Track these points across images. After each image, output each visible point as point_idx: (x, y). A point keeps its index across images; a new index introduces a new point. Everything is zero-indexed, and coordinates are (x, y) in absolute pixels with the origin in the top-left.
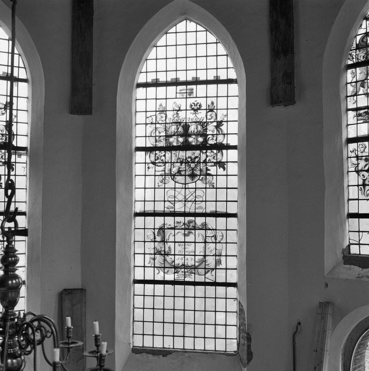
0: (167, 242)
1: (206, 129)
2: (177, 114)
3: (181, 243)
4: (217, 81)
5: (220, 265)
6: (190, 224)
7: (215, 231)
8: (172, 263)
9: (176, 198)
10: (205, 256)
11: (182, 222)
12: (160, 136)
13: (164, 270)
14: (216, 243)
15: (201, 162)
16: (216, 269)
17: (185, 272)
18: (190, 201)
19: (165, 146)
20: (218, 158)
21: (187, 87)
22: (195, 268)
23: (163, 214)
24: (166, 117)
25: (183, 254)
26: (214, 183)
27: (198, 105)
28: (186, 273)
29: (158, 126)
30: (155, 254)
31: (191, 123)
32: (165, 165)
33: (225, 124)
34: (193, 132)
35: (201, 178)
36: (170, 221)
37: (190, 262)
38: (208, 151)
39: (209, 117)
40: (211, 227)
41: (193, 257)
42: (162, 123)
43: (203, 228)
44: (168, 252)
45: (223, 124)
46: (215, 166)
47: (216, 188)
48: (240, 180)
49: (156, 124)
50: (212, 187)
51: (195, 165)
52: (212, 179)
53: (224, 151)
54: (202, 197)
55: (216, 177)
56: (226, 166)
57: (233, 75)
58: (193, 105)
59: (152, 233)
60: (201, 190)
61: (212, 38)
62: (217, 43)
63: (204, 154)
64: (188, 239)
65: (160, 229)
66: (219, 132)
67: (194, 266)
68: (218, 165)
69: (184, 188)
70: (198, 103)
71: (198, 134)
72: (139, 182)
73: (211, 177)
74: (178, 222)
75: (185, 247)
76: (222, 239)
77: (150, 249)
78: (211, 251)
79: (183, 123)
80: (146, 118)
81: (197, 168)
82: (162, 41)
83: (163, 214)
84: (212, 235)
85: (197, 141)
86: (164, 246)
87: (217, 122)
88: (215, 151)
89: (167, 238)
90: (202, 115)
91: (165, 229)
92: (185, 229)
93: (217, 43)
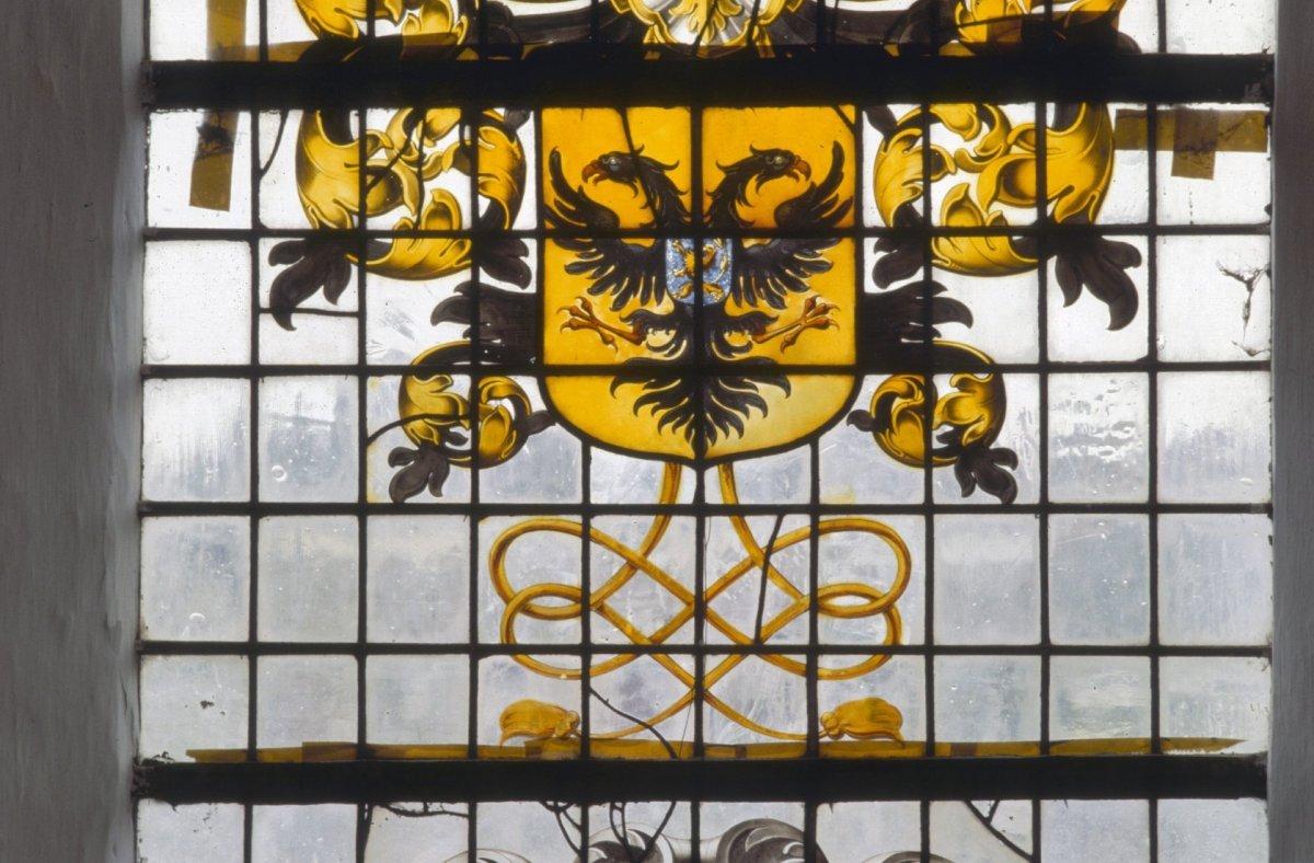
9: (594, 617)
15: (874, 232)
20: (1053, 188)
26: (1009, 457)
35: (864, 403)
56: (1138, 276)
68: (1052, 264)
69: (683, 510)
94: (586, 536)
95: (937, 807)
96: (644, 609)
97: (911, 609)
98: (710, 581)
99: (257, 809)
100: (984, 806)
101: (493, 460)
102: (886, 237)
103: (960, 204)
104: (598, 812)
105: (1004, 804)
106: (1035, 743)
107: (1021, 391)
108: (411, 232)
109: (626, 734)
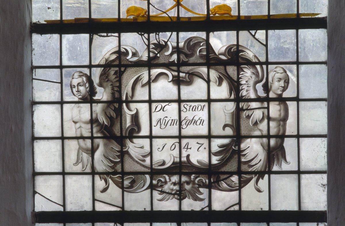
7: (264, 67)
10: (238, 137)
16: (270, 172)
28: (187, 187)
30: (92, 138)
40: (255, 56)
59: (84, 79)
64: (187, 92)
65: (107, 65)
76: (285, 89)
77: (78, 125)
89: (127, 89)
95: (241, 33)
99: (63, 35)
100: (253, 32)
104: (152, 35)
105: (258, 31)
106: (266, 15)
109: (159, 15)
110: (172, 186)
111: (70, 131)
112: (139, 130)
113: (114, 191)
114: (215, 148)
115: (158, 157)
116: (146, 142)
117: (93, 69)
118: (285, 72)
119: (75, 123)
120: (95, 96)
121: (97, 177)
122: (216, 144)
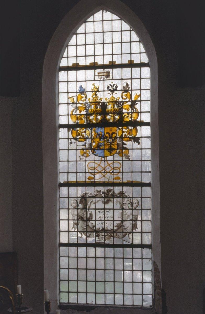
0: (89, 209)
1: (122, 108)
2: (96, 95)
3: (101, 210)
4: (131, 65)
5: (136, 229)
6: (109, 193)
7: (131, 199)
8: (93, 228)
9: (96, 170)
11: (102, 191)
12: (81, 115)
13: (86, 234)
14: (132, 209)
15: (118, 138)
16: (133, 232)
17: (105, 236)
18: (109, 172)
19: (85, 123)
21: (104, 70)
22: (113, 231)
23: (85, 184)
24: (86, 97)
25: (103, 219)
26: (130, 156)
27: (115, 86)
28: (106, 237)
29: (79, 105)
30: (78, 220)
31: (108, 102)
32: (86, 140)
33: (139, 103)
34: (110, 110)
35: (117, 152)
36: (91, 190)
37: (109, 226)
38: (124, 127)
39: (124, 97)
41: (112, 222)
42: (82, 103)
43: (121, 196)
44: (90, 218)
45: (137, 104)
46: (131, 141)
47: (132, 161)
48: (154, 215)
49: (77, 103)
50: (128, 160)
51: (113, 140)
52: (127, 152)
53: (139, 128)
54: (119, 168)
55: (131, 150)
56: (140, 141)
57: (145, 59)
58: (110, 86)
59: (75, 201)
60: (118, 162)
61: (126, 26)
62: (130, 30)
63: (120, 130)
64: (107, 206)
66: (134, 110)
67: (113, 230)
68: (133, 140)
69: (103, 161)
70: (114, 85)
71: (114, 113)
72: (62, 155)
73: (127, 150)
74: (98, 192)
75: (105, 213)
76: (137, 206)
77: (73, 216)
78: (128, 217)
79: (101, 102)
80: (68, 98)
81: (115, 143)
82: (81, 29)
83: (85, 184)
84: (128, 202)
85: (114, 118)
86: (86, 212)
87: (132, 101)
88: (130, 128)
89: (88, 205)
90: (118, 95)
91: (86, 197)
92: (104, 197)
93: (130, 30)
94: (95, 163)
96: (100, 169)
97: (121, 169)
98: (105, 167)
101: (87, 157)
102: (119, 138)
103: (125, 135)
107: (130, 151)
108: (80, 138)
110: (102, 237)
111: (71, 218)
112: (92, 218)
113: (84, 236)
114: (115, 225)
115: (97, 227)
116: (94, 222)
117: (78, 198)
118: (138, 201)
119: (72, 215)
120: (78, 207)
121: (79, 233)
122: (116, 223)
